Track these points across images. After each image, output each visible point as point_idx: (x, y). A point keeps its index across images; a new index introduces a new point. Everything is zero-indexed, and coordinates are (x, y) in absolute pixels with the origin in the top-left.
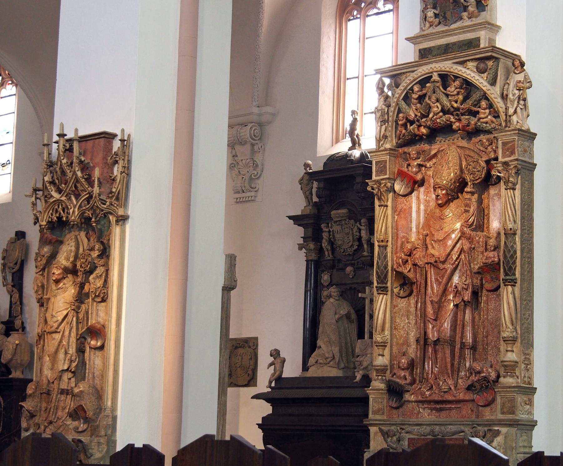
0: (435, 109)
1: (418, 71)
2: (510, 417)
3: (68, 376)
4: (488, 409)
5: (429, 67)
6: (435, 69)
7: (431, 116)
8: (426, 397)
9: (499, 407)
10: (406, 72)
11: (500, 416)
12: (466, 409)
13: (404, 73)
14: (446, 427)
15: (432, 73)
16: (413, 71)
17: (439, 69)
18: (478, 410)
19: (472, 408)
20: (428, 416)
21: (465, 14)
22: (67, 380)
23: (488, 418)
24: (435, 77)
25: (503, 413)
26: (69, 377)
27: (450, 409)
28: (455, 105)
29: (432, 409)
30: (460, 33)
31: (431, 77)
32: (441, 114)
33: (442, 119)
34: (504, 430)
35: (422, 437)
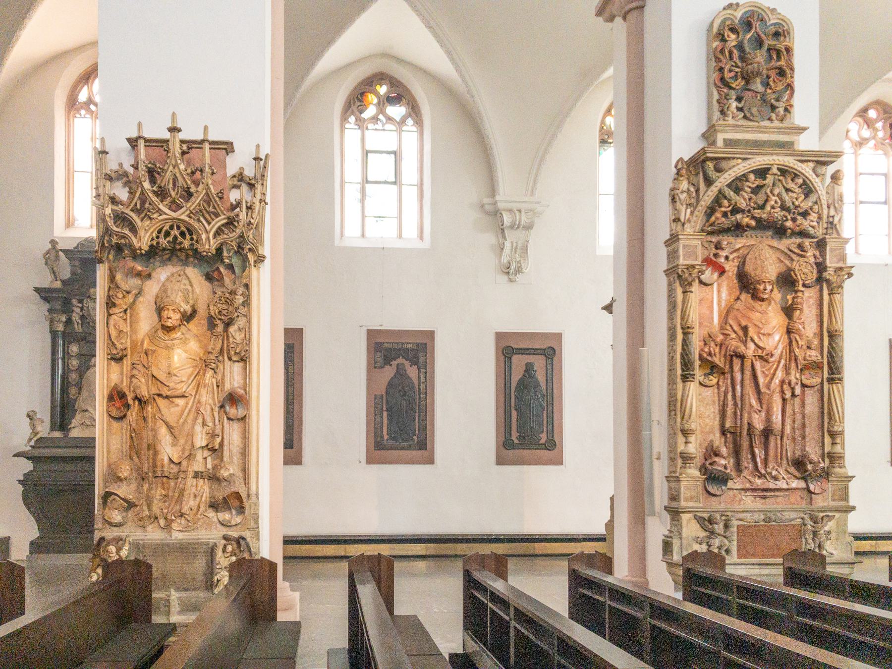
0: (773, 203)
1: (754, 160)
2: (843, 503)
3: (203, 455)
4: (820, 497)
5: (771, 158)
6: (777, 162)
7: (768, 208)
8: (758, 485)
9: (830, 495)
10: (738, 158)
11: (833, 504)
12: (795, 497)
13: (734, 158)
14: (784, 513)
15: (772, 165)
16: (744, 159)
17: (782, 163)
18: (811, 499)
19: (802, 496)
20: (752, 502)
21: (773, 116)
22: (201, 460)
23: (821, 504)
24: (775, 170)
25: (833, 500)
26: (204, 456)
27: (777, 496)
28: (797, 203)
29: (755, 497)
30: (773, 133)
31: (769, 169)
32: (779, 209)
33: (778, 214)
34: (837, 515)
35: (754, 524)
